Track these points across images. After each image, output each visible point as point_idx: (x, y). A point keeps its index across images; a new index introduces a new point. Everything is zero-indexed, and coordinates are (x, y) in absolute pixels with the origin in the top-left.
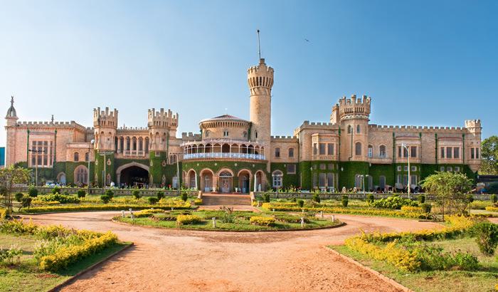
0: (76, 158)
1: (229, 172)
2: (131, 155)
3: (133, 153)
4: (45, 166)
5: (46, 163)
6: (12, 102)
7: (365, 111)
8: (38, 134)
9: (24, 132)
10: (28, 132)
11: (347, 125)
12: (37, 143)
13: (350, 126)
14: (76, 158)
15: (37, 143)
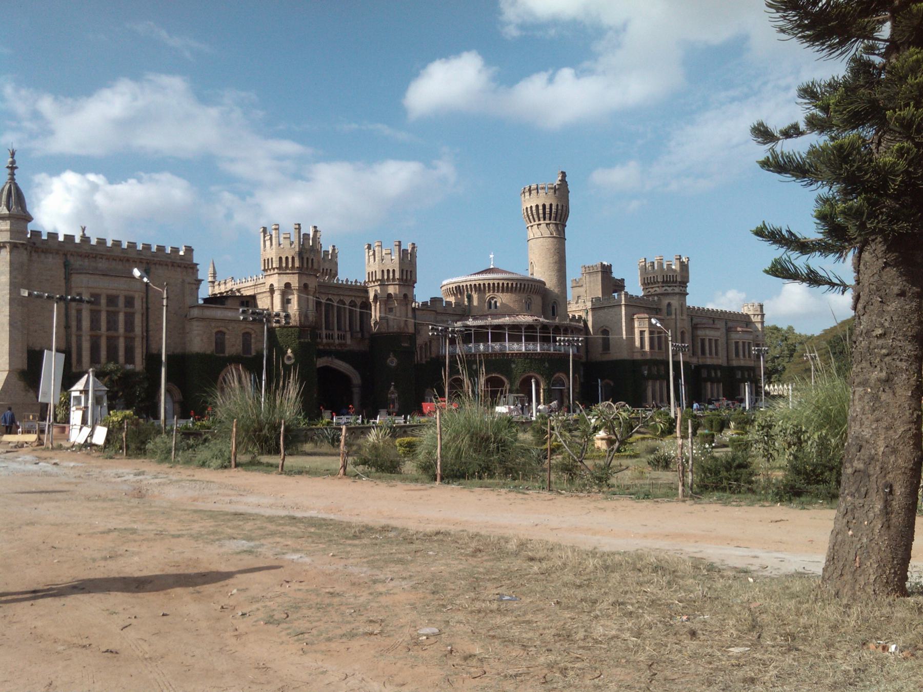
0: (220, 344)
1: (561, 380)
2: (337, 341)
3: (328, 337)
4: (129, 367)
5: (130, 358)
6: (12, 168)
7: (679, 279)
8: (95, 272)
9: (54, 263)
10: (66, 265)
11: (665, 302)
12: (103, 301)
13: (669, 305)
14: (220, 344)
15: (103, 301)
